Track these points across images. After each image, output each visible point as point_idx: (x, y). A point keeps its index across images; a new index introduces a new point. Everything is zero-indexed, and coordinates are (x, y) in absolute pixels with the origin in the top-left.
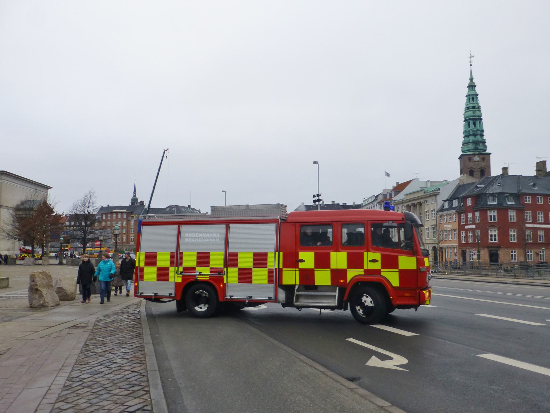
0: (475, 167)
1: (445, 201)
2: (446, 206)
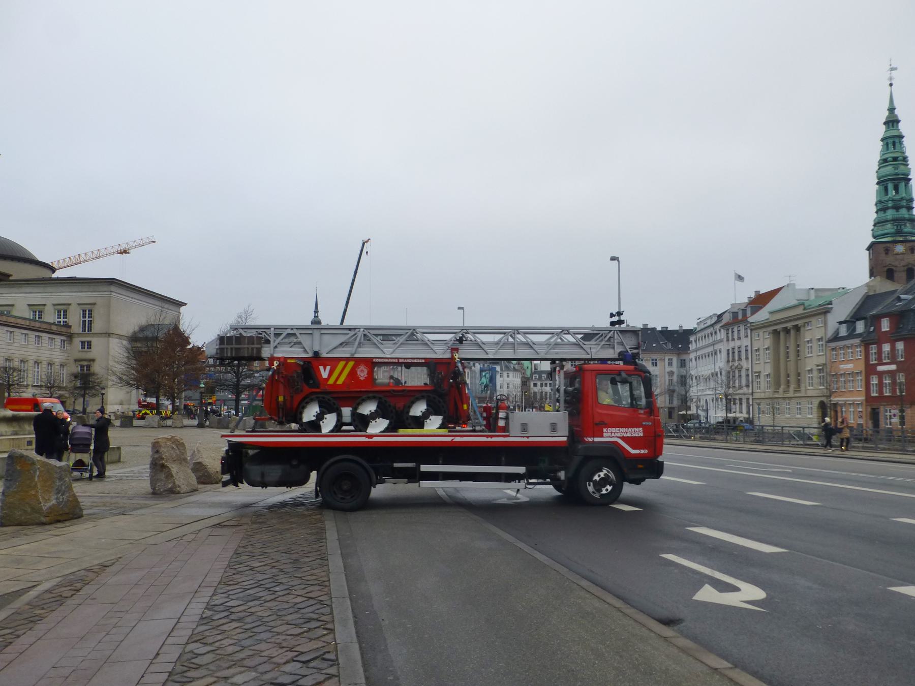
0: (896, 263)
1: (840, 323)
2: (843, 331)
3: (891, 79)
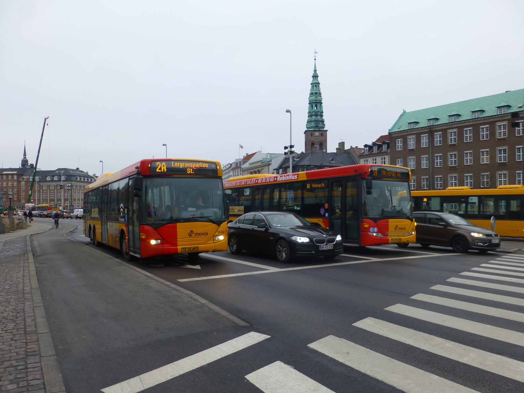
0: (315, 140)
1: (274, 170)
3: (315, 57)
